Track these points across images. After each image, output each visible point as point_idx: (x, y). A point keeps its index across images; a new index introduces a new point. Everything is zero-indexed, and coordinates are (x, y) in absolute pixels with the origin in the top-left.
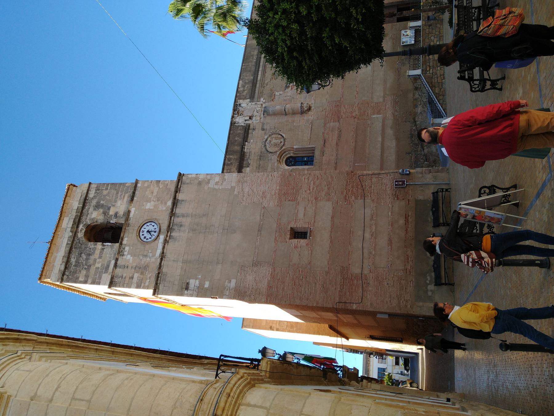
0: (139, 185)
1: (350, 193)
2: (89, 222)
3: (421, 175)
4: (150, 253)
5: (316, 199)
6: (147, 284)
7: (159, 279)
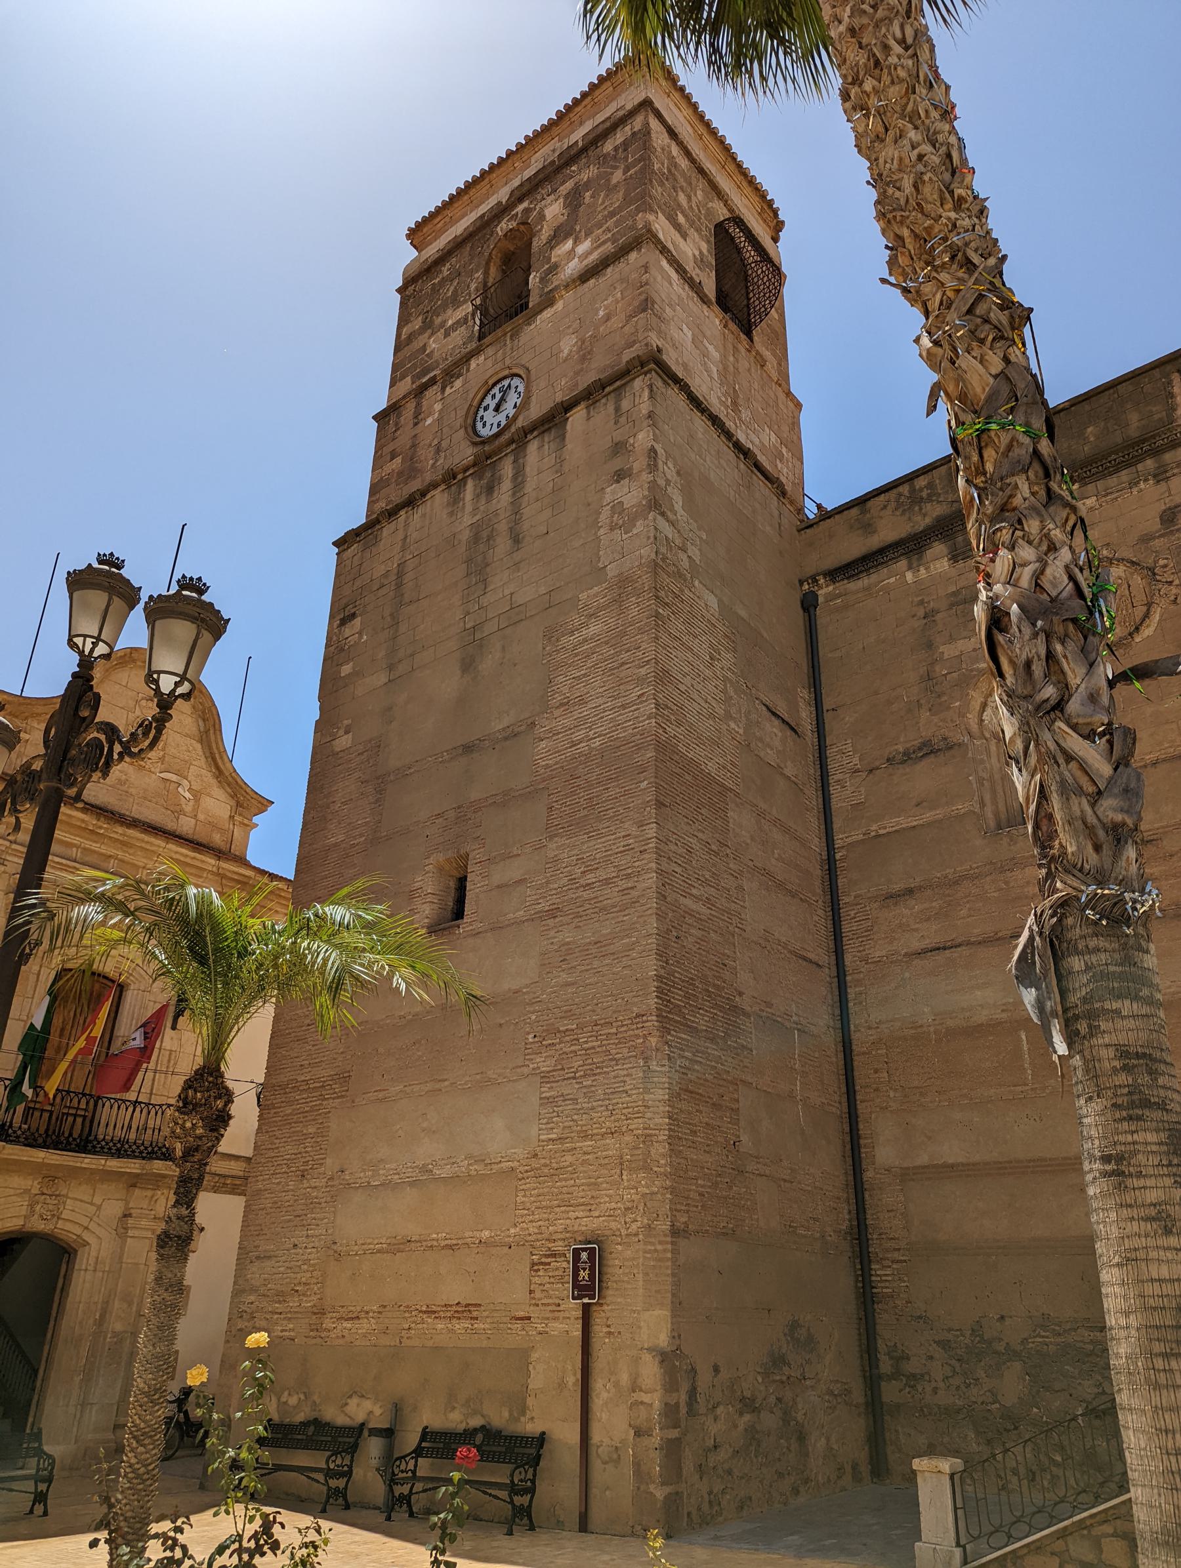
3: (625, 1378)
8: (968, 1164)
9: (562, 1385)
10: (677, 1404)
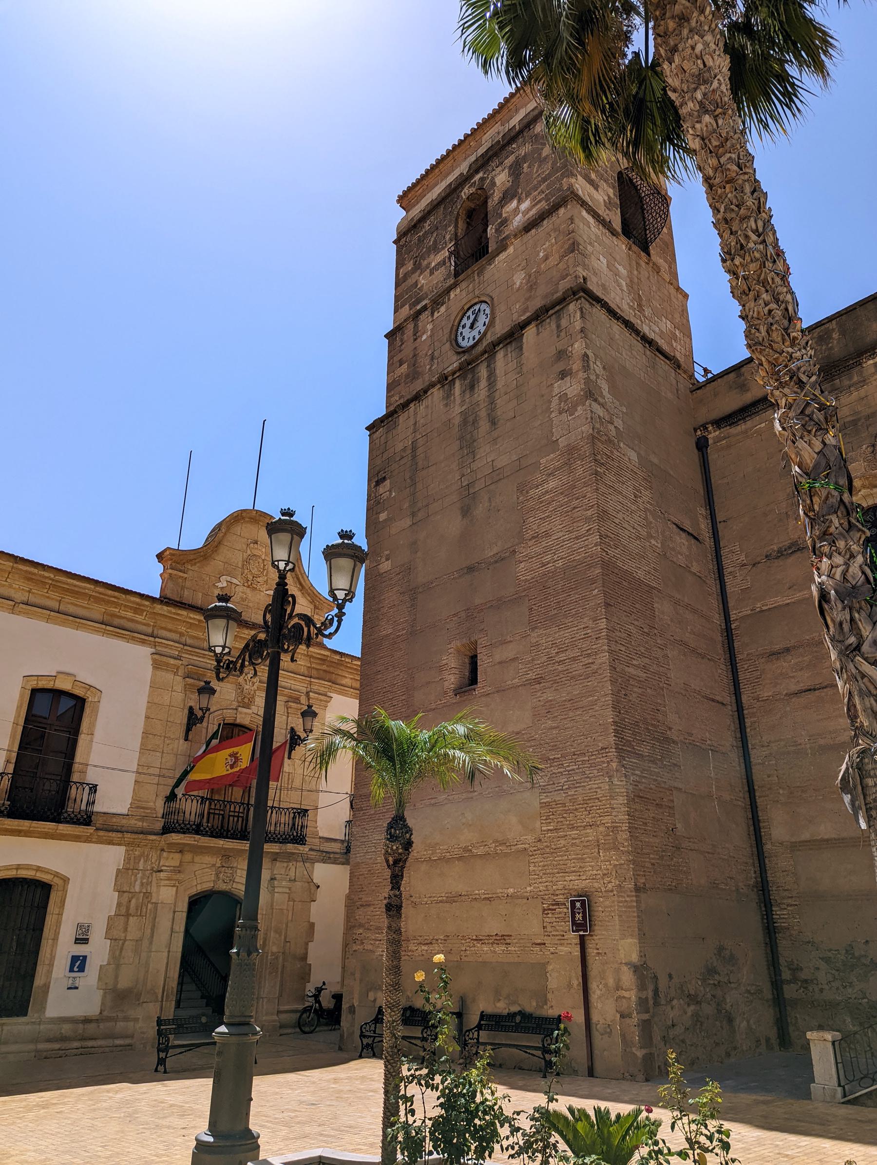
3: (611, 982)
8: (839, 839)
9: (570, 986)
10: (647, 998)
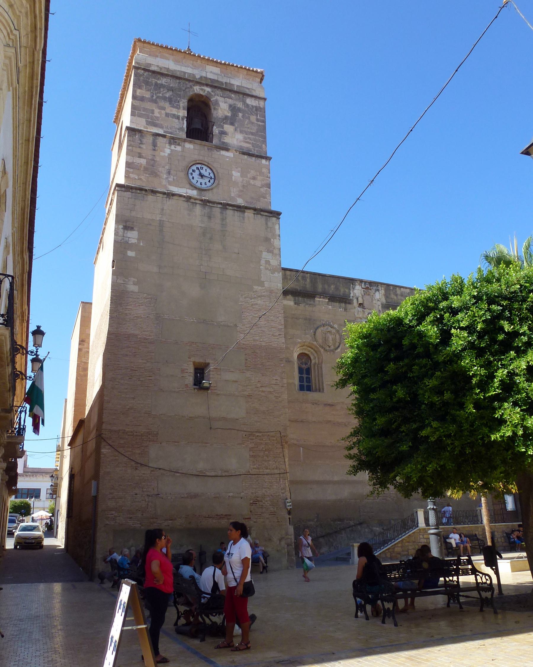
0: (264, 161)
1: (259, 441)
2: (214, 99)
4: (174, 179)
5: (249, 396)
6: (132, 176)
7: (138, 191)
